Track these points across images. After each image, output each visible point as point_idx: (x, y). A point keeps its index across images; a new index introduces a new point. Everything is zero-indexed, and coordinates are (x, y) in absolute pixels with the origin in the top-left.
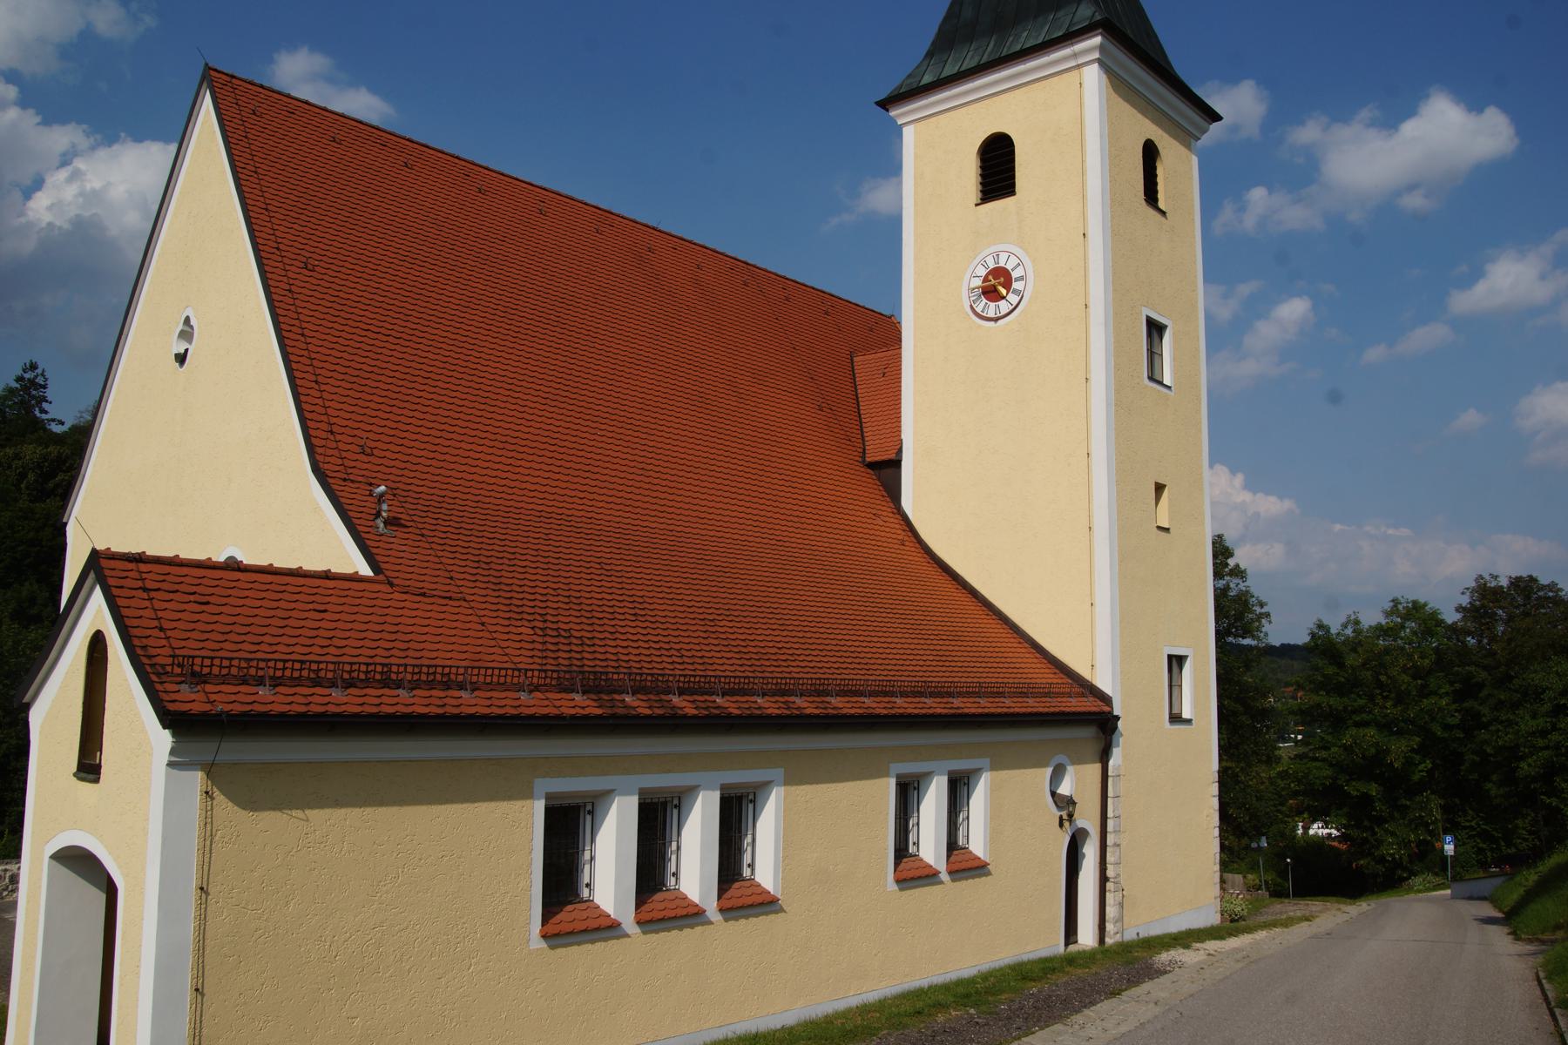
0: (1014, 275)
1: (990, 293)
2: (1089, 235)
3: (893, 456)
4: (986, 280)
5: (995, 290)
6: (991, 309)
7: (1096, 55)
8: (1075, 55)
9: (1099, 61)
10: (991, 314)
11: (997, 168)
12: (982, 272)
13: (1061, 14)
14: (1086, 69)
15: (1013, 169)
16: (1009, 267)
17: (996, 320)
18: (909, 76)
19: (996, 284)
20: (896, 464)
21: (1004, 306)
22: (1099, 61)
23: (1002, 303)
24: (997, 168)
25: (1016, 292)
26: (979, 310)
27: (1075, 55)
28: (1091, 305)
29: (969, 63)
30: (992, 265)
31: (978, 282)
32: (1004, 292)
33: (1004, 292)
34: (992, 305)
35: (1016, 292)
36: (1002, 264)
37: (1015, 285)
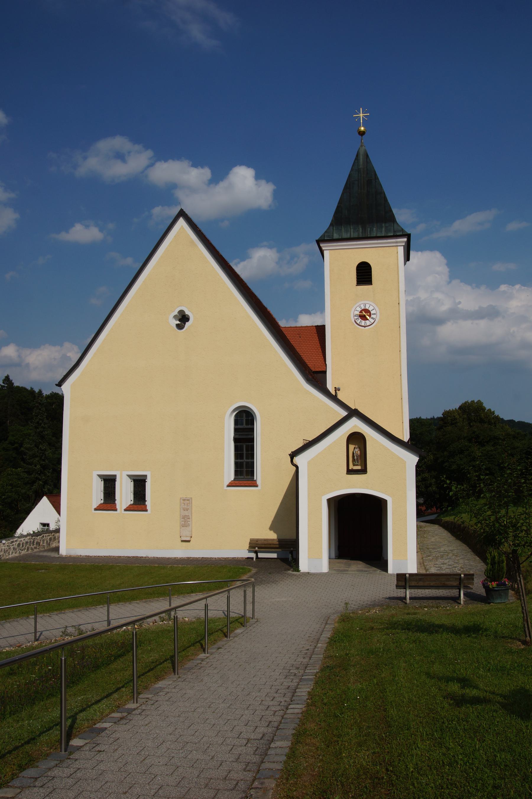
0: (372, 312)
1: (363, 317)
2: (400, 303)
3: (323, 370)
4: (361, 312)
5: (364, 316)
6: (363, 323)
7: (404, 244)
8: (397, 242)
9: (404, 246)
10: (363, 324)
11: (364, 273)
12: (360, 310)
13: (387, 225)
14: (399, 247)
15: (371, 275)
16: (370, 309)
17: (365, 327)
18: (326, 232)
19: (364, 314)
20: (325, 372)
21: (368, 323)
22: (404, 246)
23: (367, 321)
24: (364, 273)
25: (372, 318)
26: (358, 322)
27: (397, 242)
28: (401, 327)
29: (356, 235)
30: (363, 308)
31: (358, 313)
32: (368, 317)
33: (368, 317)
34: (363, 321)
35: (372, 318)
36: (367, 308)
37: (372, 316)
